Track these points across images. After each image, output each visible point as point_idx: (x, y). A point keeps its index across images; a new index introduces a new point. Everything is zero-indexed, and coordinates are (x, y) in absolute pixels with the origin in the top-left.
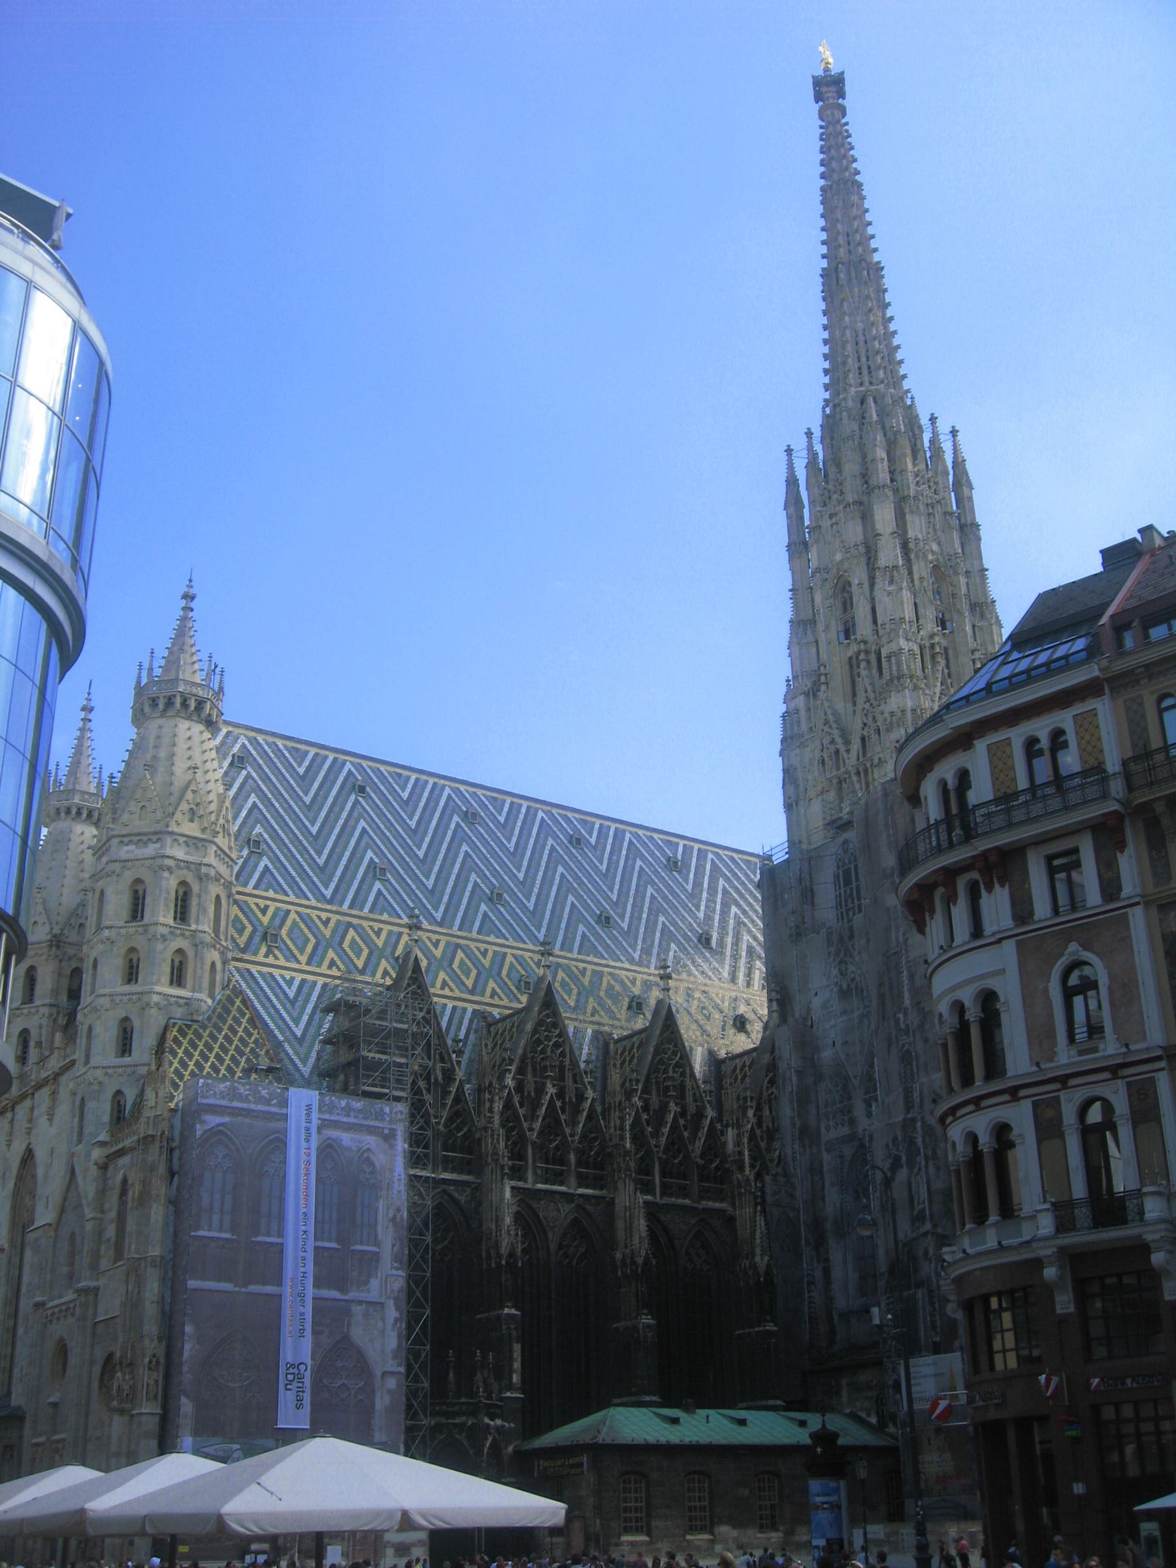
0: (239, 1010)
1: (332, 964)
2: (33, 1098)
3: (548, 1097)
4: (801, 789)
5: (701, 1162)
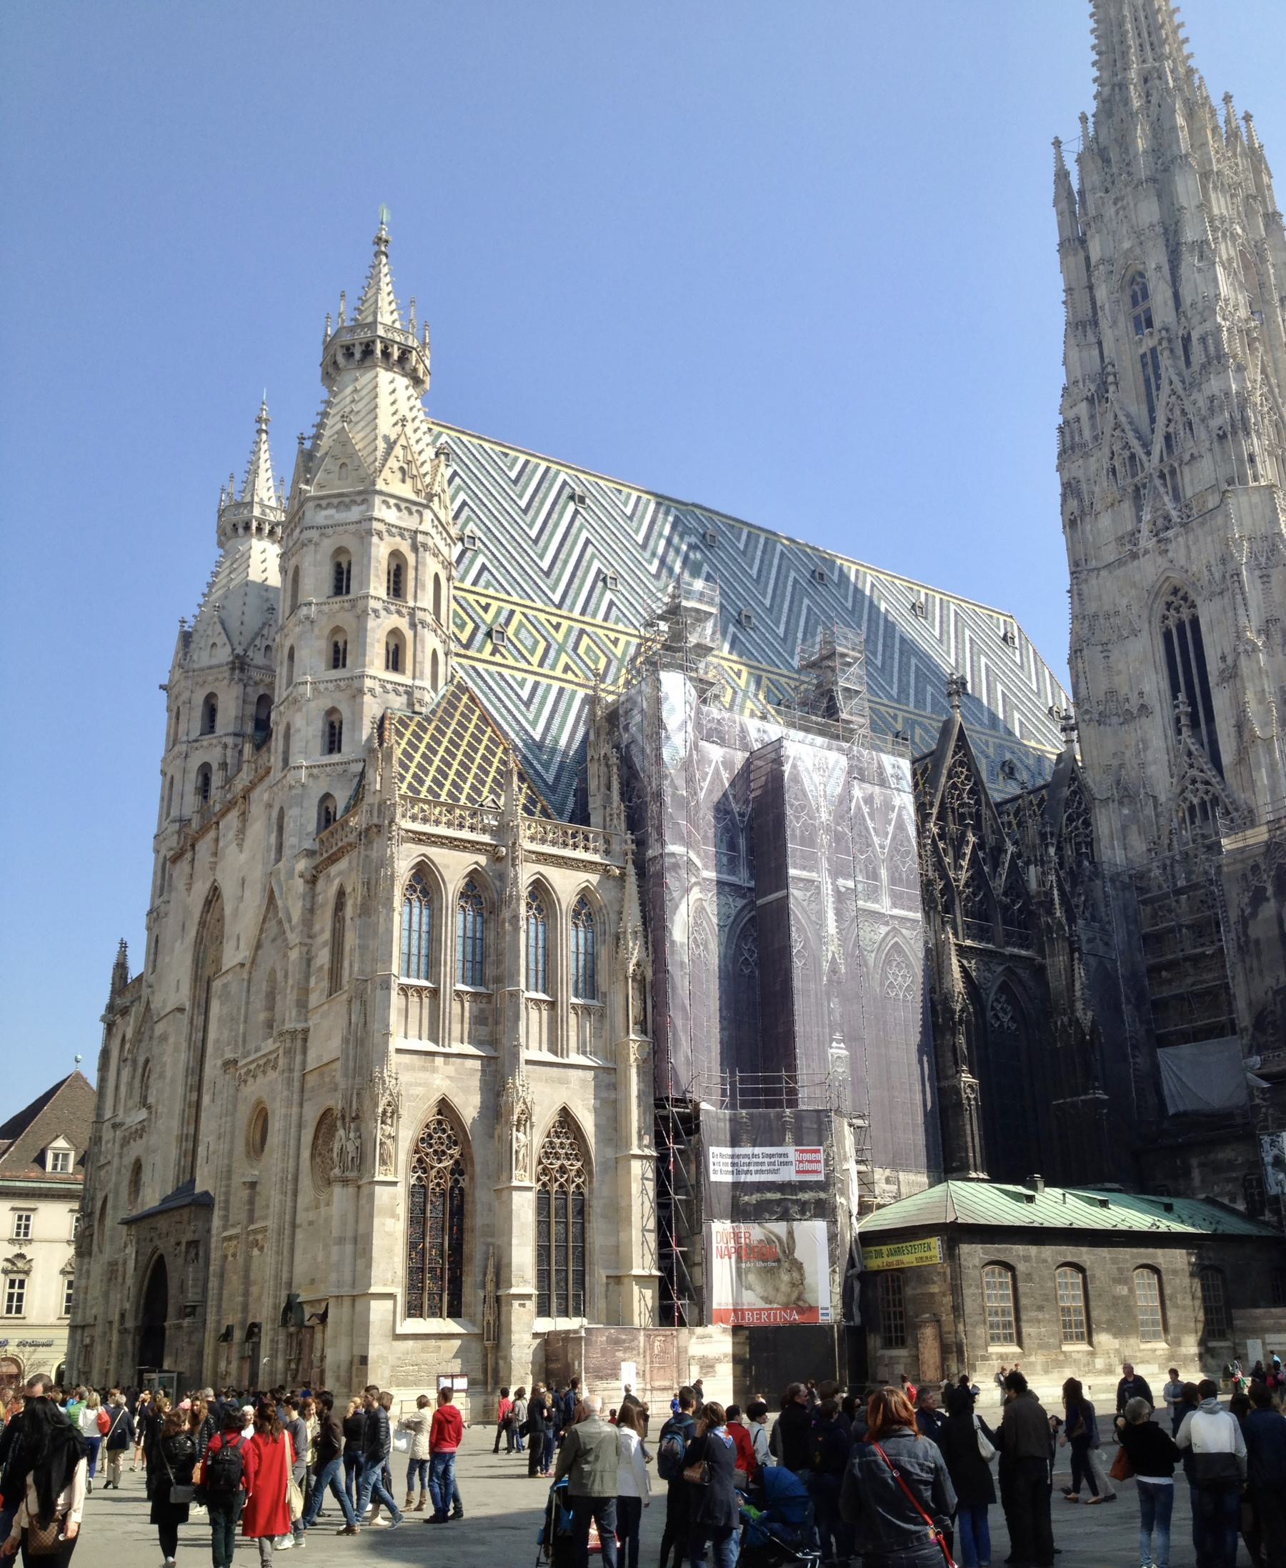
0: (466, 706)
2: (218, 829)
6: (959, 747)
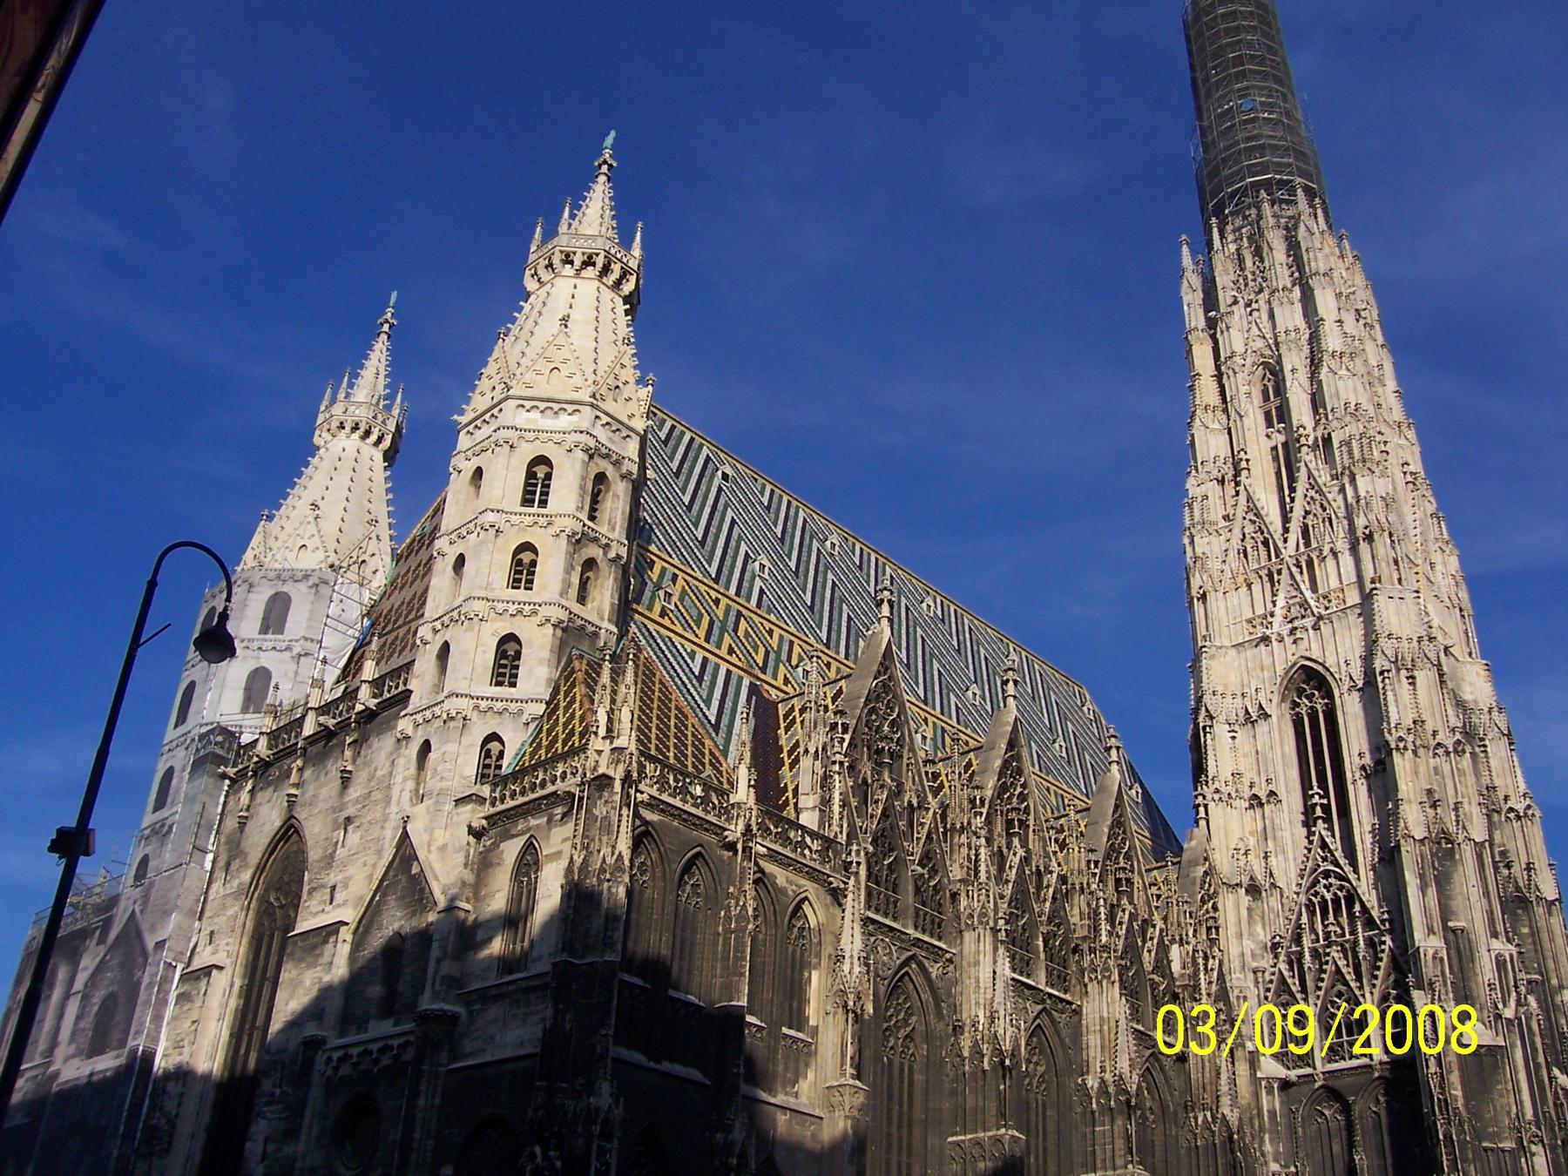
1: (731, 651)
3: (1017, 860)
4: (1216, 580)
5: (1155, 977)
6: (1117, 807)
